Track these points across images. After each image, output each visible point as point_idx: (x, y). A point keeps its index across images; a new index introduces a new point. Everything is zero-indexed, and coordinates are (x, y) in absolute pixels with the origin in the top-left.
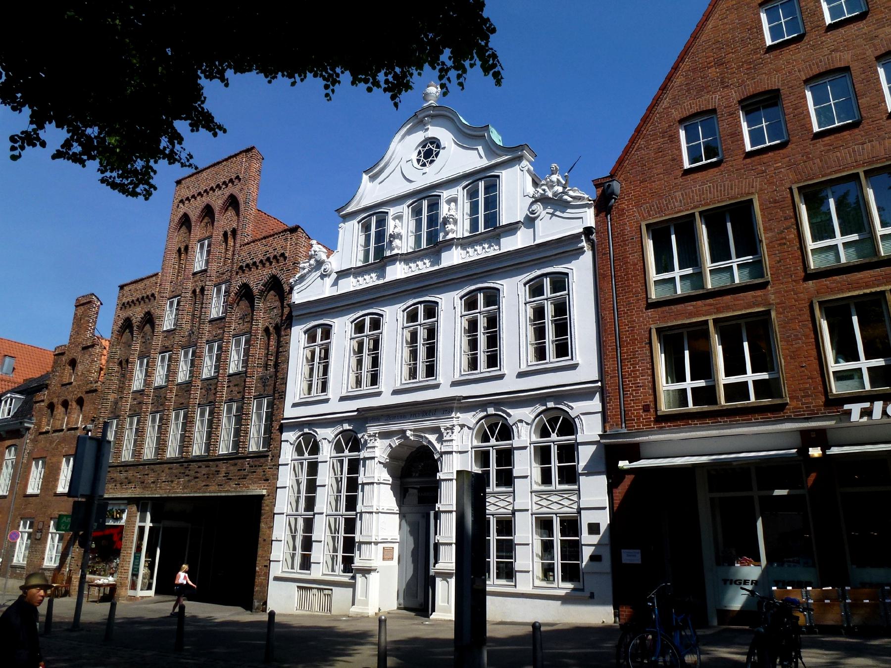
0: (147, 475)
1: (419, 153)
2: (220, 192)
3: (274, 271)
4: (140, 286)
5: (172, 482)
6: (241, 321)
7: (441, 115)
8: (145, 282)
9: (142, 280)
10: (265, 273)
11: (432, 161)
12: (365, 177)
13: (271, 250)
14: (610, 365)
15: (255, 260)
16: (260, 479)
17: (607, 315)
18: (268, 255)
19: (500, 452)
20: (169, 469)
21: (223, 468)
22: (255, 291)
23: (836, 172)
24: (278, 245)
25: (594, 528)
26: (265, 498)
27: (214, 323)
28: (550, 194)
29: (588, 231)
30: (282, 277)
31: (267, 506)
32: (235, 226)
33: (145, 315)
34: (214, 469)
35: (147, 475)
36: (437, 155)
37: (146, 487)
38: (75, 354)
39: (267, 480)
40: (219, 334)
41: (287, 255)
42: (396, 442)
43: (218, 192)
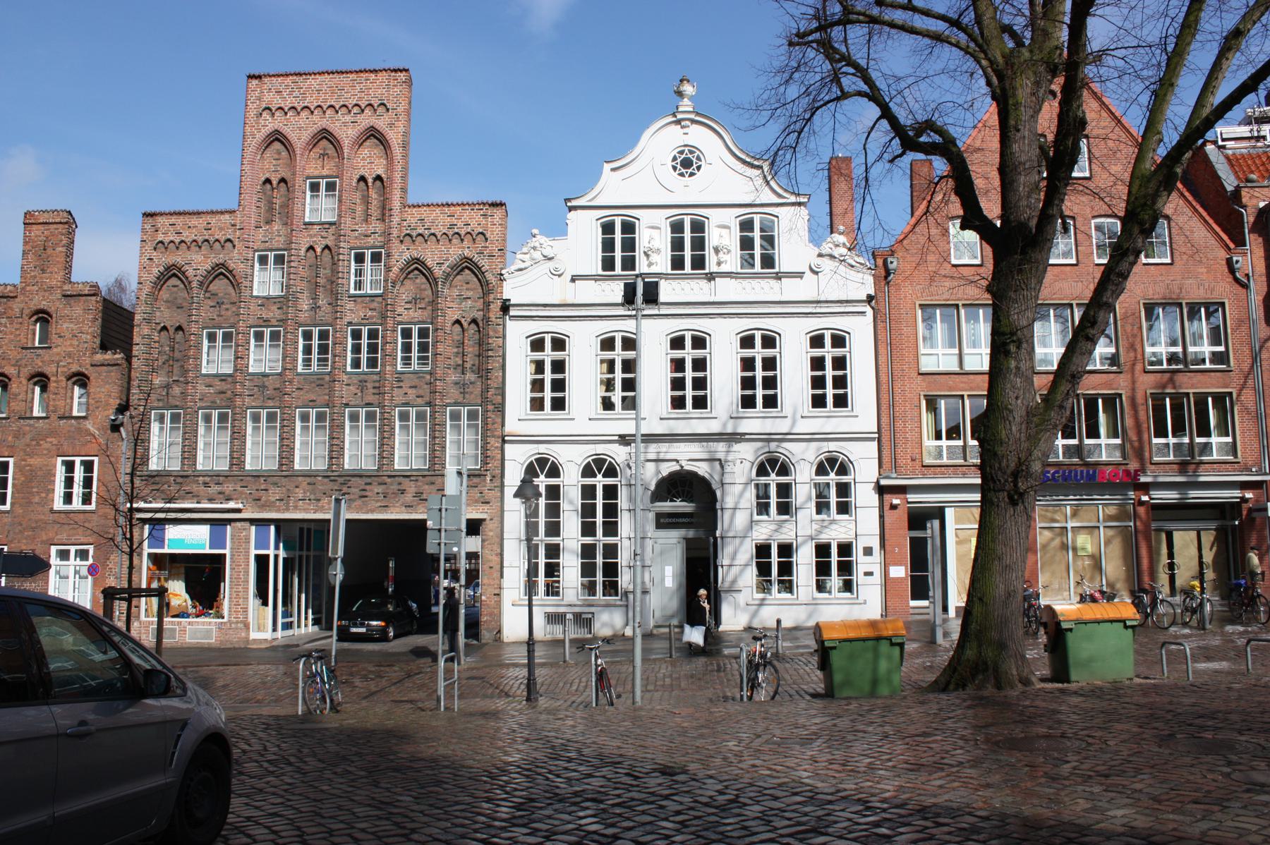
0: (266, 490)
1: (675, 159)
2: (348, 118)
3: (467, 253)
4: (194, 221)
5: (319, 500)
6: (408, 306)
7: (701, 118)
8: (209, 218)
9: (198, 213)
10: (455, 252)
11: (692, 175)
12: (607, 167)
13: (460, 224)
14: (884, 420)
15: (433, 231)
16: (476, 501)
17: (883, 378)
18: (456, 230)
19: (779, 486)
20: (309, 484)
21: (411, 488)
22: (438, 272)
23: (1060, 299)
24: (474, 220)
25: (868, 551)
26: (487, 522)
27: (359, 300)
28: (836, 253)
29: (870, 299)
30: (484, 263)
31: (491, 531)
32: (381, 172)
33: (213, 268)
34: (395, 487)
35: (266, 490)
36: (699, 168)
37: (263, 506)
38: (44, 303)
39: (488, 503)
40: (372, 317)
41: (488, 236)
42: (667, 469)
43: (343, 117)
